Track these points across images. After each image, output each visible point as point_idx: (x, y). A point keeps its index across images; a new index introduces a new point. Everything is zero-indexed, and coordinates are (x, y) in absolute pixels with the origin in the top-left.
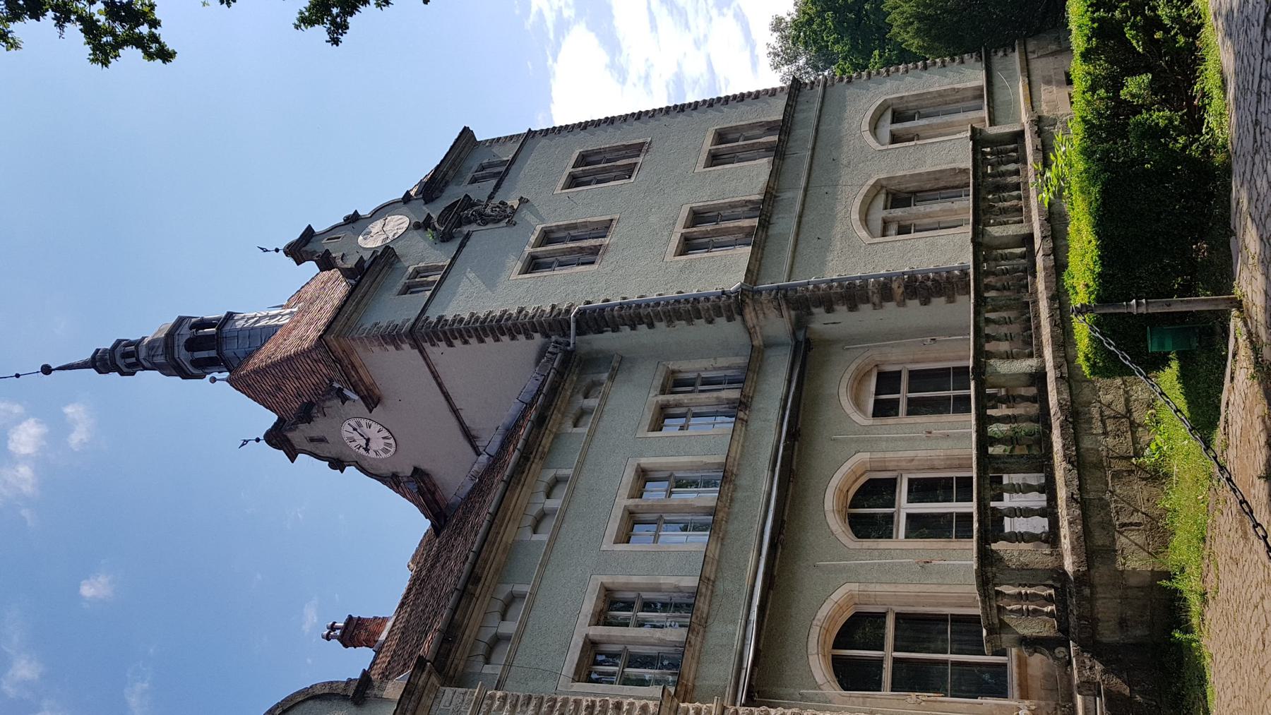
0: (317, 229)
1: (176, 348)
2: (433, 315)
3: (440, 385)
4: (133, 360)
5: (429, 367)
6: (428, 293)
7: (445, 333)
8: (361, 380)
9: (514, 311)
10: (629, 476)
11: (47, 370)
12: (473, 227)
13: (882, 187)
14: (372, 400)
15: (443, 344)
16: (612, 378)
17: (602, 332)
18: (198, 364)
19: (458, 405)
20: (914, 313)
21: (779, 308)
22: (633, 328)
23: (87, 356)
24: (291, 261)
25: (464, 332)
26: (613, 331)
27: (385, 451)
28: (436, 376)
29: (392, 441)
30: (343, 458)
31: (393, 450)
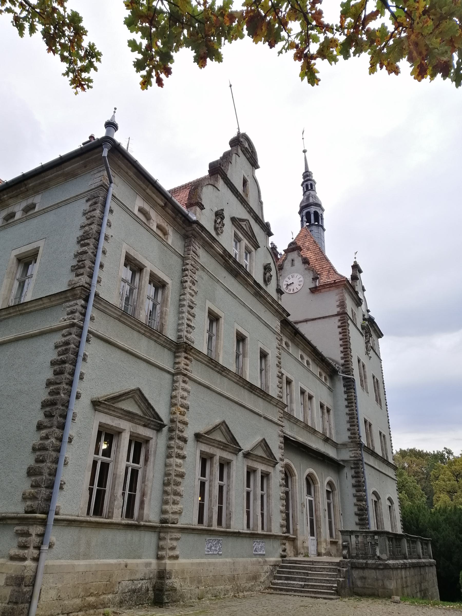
0: (361, 274)
1: (315, 207)
2: (349, 322)
3: (320, 318)
4: (310, 188)
5: (329, 316)
10: (312, 393)
13: (378, 500)
14: (314, 290)
15: (339, 324)
16: (329, 388)
17: (344, 386)
18: (308, 214)
20: (351, 509)
21: (355, 457)
22: (346, 400)
23: (310, 169)
24: (352, 264)
26: (345, 391)
28: (324, 318)
29: (291, 292)
30: (283, 270)
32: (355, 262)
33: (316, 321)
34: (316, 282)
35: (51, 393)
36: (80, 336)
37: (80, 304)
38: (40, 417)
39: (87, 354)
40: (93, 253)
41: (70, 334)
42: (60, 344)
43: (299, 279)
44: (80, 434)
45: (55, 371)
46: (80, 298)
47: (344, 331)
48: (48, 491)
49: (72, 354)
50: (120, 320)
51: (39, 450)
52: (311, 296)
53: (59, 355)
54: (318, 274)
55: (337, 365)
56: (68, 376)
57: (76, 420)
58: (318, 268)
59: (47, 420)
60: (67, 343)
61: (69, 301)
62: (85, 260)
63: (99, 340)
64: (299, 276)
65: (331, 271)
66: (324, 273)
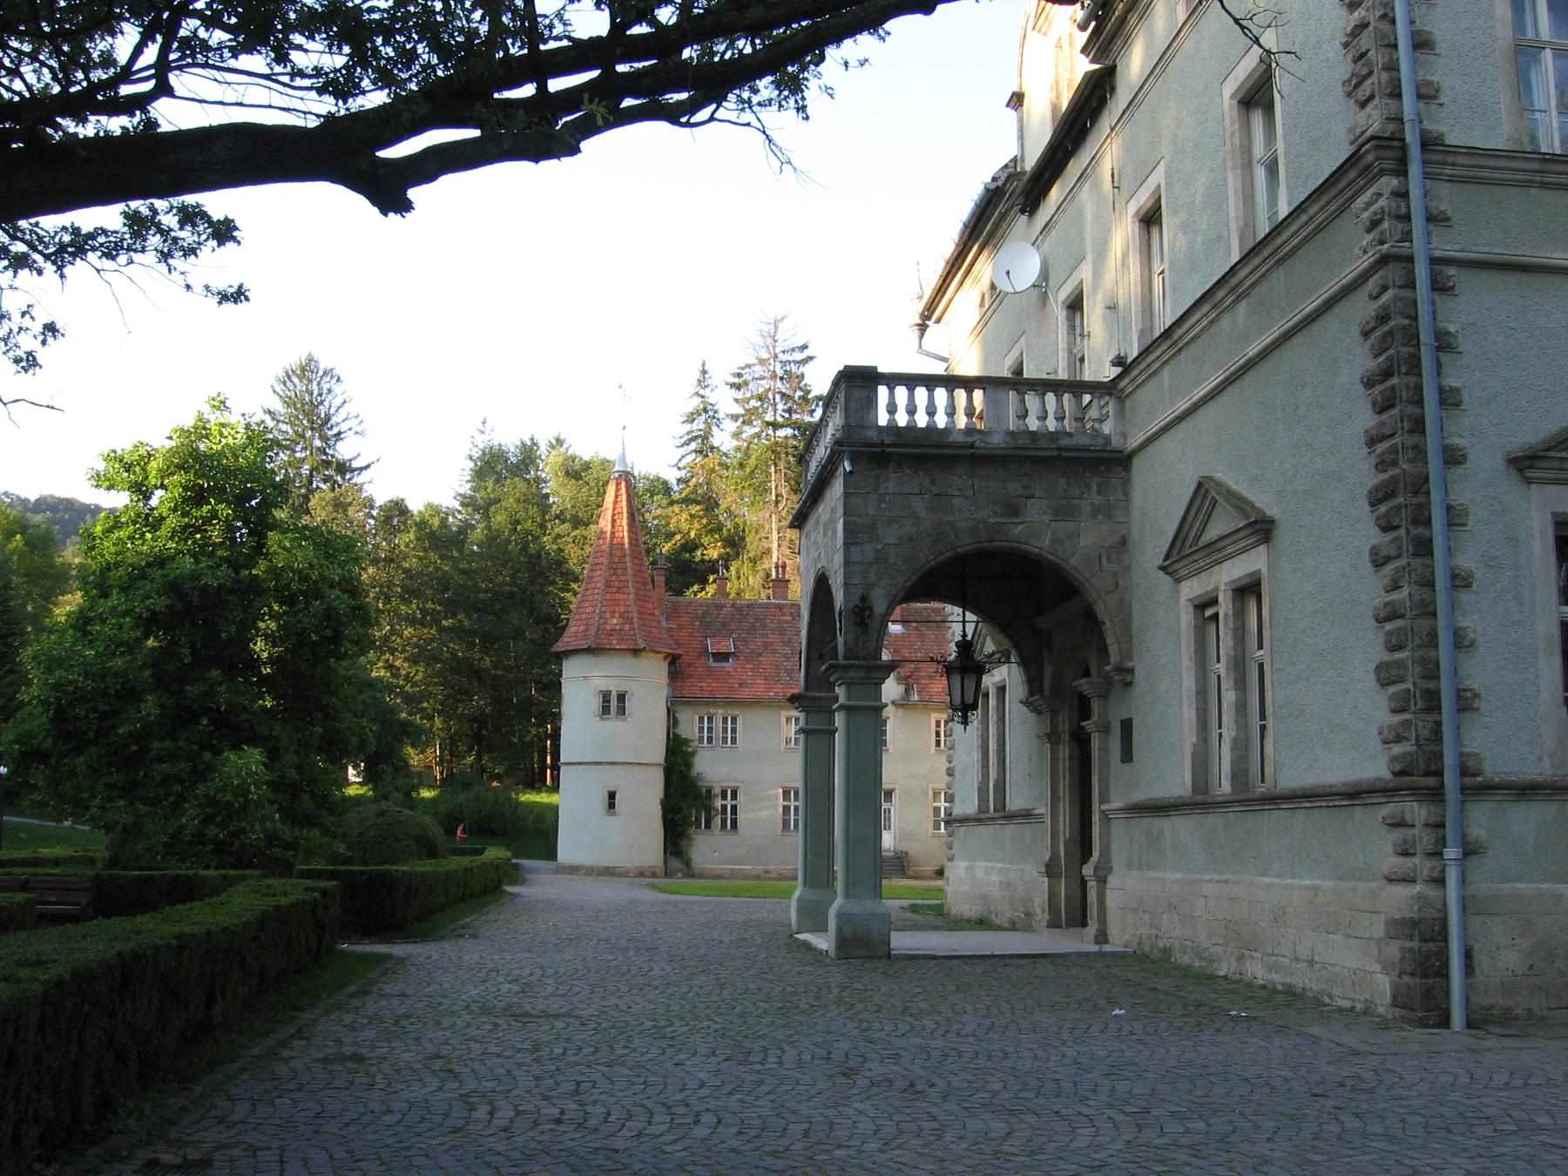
35: (1381, 465)
36: (1411, 284)
37: (1387, 192)
38: (1374, 536)
39: (1452, 328)
40: (1383, 17)
41: (1385, 288)
42: (1371, 326)
44: (1492, 558)
45: (1374, 404)
46: (1382, 173)
48: (1430, 718)
49: (1403, 345)
50: (1543, 186)
51: (1388, 619)
53: (1376, 356)
56: (1410, 410)
57: (1470, 522)
59: (1388, 537)
60: (1383, 318)
61: (1362, 190)
62: (1367, 51)
63: (1283, 348)
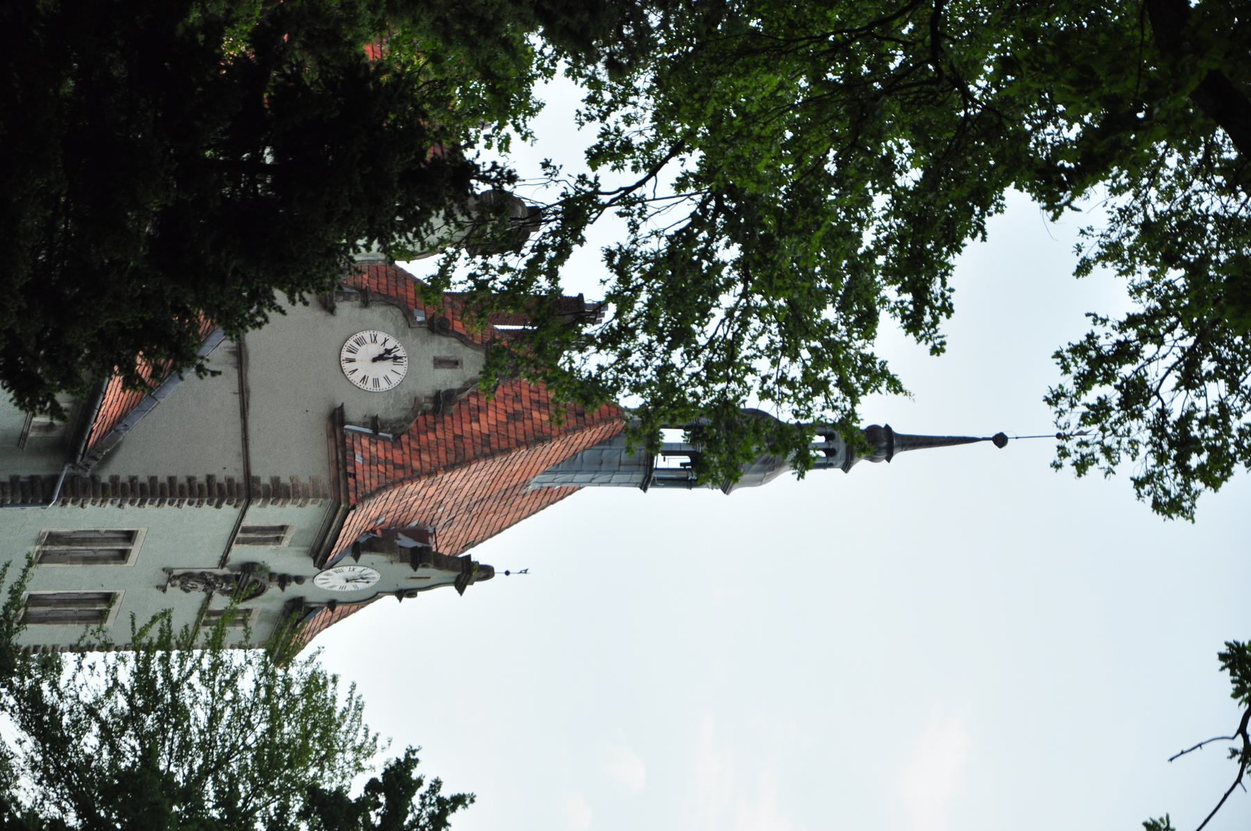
0: (452, 590)
2: (228, 513)
6: (247, 522)
7: (210, 493)
8: (337, 447)
9: (127, 505)
11: (1000, 440)
12: (219, 572)
14: (337, 418)
15: (220, 478)
16: (24, 436)
17: (33, 479)
19: (235, 401)
23: (900, 457)
25: (187, 492)
27: (360, 342)
29: (345, 355)
31: (351, 342)
32: (487, 572)
33: (238, 418)
34: (365, 425)
43: (386, 378)
47: (197, 490)
52: (323, 410)
54: (397, 438)
55: (94, 464)
58: (423, 438)
64: (395, 379)
65: (400, 474)
66: (397, 453)
